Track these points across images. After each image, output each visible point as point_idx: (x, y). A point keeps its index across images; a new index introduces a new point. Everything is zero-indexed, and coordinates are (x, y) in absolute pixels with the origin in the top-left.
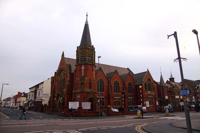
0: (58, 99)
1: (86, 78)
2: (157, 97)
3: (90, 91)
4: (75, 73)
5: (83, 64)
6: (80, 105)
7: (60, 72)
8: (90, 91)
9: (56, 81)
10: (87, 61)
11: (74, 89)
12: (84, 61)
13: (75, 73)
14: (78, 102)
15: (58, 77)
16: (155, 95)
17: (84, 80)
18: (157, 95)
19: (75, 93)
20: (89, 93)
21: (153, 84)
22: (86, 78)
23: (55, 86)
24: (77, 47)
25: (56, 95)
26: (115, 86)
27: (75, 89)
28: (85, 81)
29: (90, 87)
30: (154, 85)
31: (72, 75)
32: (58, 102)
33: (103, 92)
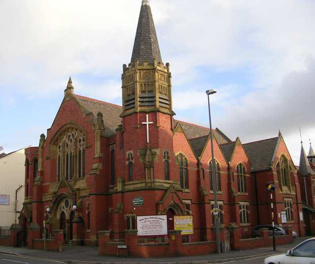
0: (57, 208)
1: (158, 151)
2: (300, 201)
3: (168, 185)
4: (118, 137)
5: (148, 113)
6: (171, 225)
7: (61, 135)
8: (168, 185)
9: (48, 158)
10: (158, 104)
11: (119, 179)
12: (150, 104)
13: (118, 137)
14: (165, 217)
15: (53, 148)
16: (296, 195)
17: (153, 154)
18: (299, 196)
19: (122, 192)
20: (166, 190)
21: (291, 169)
22: (158, 151)
23: (42, 173)
24: (124, 66)
25: (48, 197)
26: (238, 176)
27: (123, 182)
28: (156, 159)
29: (167, 177)
30: (293, 171)
31: (107, 141)
32: (58, 217)
33: (188, 188)
